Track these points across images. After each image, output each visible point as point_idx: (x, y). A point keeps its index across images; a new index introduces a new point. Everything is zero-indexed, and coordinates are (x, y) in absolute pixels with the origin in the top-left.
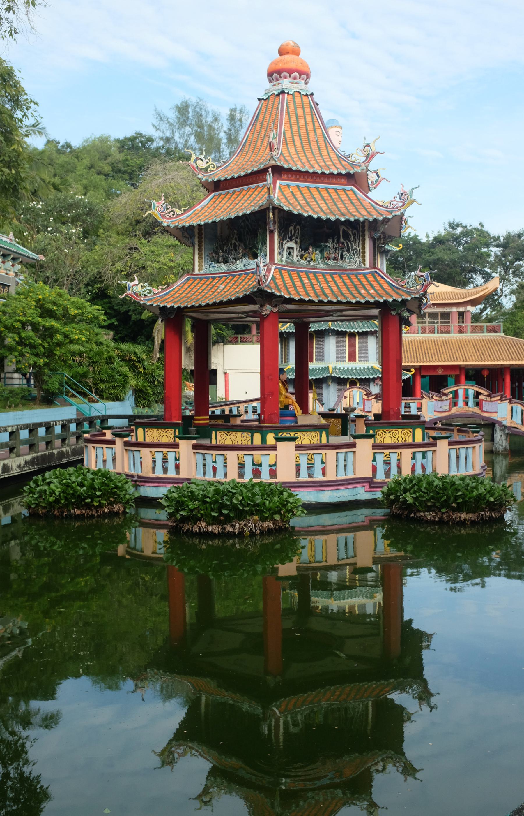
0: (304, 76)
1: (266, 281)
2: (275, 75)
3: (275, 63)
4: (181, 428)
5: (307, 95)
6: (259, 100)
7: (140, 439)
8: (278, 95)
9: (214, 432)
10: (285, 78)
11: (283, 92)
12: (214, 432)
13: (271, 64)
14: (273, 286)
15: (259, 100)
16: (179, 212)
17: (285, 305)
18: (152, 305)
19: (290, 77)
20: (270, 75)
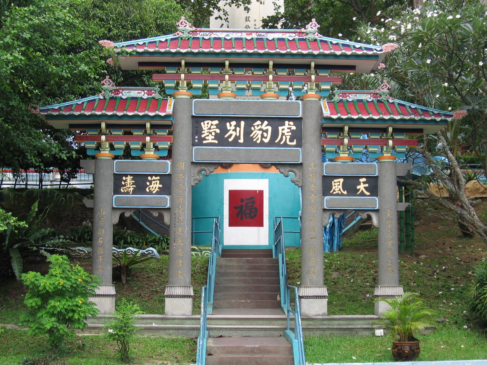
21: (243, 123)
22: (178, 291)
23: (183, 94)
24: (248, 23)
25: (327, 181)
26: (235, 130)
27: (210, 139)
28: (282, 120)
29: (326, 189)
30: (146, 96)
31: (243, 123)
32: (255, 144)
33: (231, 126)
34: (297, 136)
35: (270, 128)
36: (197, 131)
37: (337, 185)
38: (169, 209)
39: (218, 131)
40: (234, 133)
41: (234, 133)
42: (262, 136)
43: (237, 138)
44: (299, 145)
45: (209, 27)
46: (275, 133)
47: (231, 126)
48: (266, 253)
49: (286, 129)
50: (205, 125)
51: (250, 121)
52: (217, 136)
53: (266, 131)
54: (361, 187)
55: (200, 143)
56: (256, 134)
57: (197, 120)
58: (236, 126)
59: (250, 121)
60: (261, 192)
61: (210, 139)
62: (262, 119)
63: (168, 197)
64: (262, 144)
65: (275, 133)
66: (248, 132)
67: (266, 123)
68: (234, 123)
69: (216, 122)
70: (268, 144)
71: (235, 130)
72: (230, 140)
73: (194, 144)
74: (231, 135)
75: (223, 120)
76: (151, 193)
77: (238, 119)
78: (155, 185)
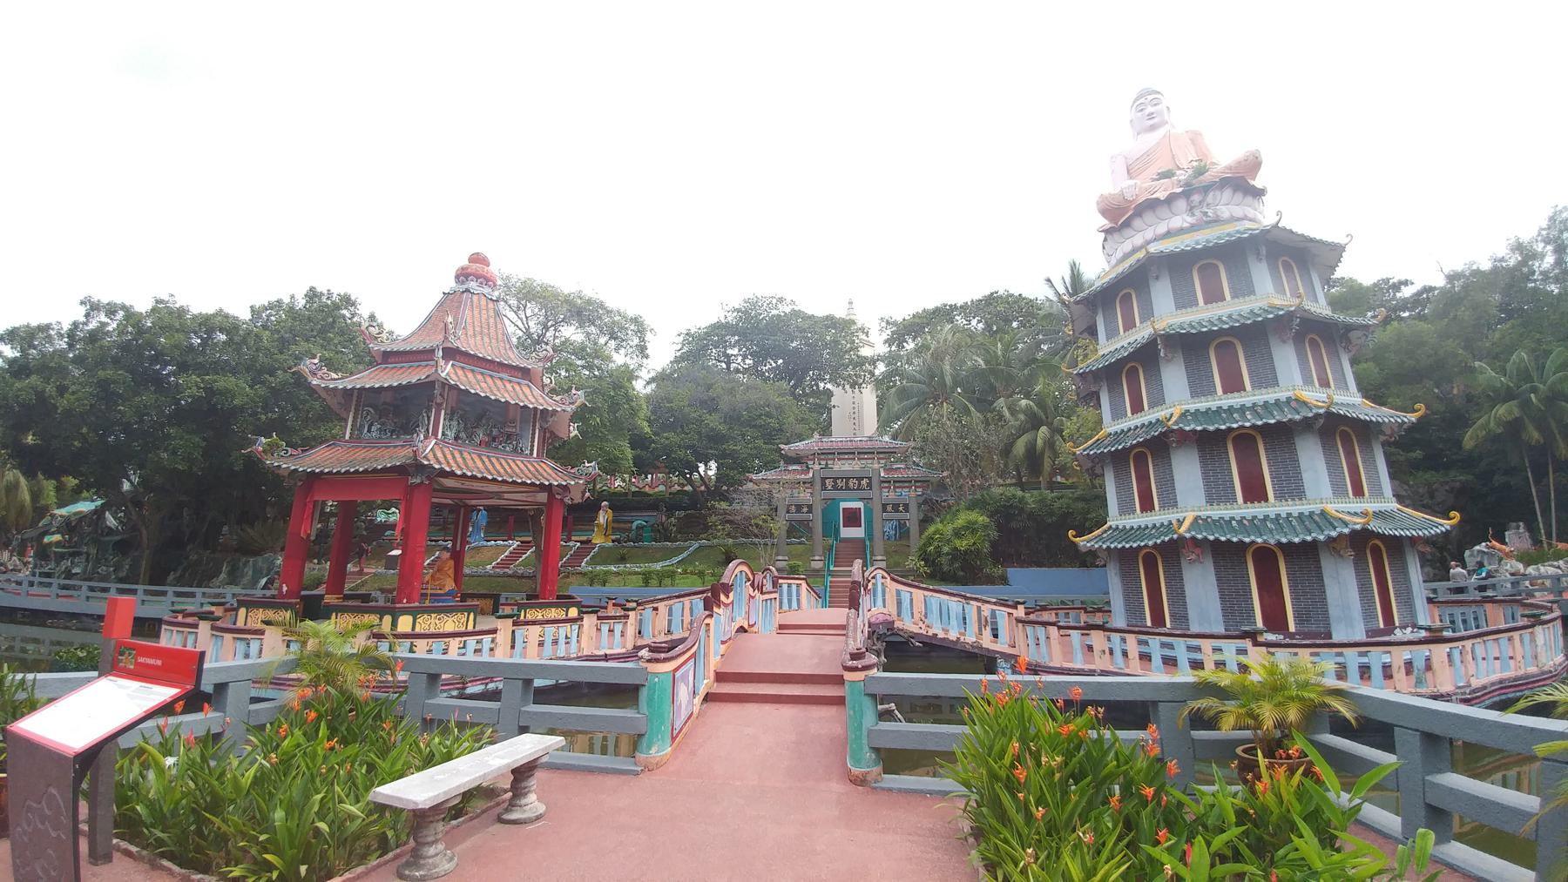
1: (425, 451)
5: (491, 299)
6: (444, 293)
7: (240, 624)
8: (463, 292)
9: (334, 614)
11: (467, 290)
12: (334, 614)
14: (431, 456)
15: (444, 293)
16: (336, 377)
17: (440, 479)
18: (279, 466)
20: (457, 277)
22: (817, 558)
23: (817, 467)
25: (884, 507)
27: (830, 488)
28: (862, 478)
29: (884, 510)
33: (839, 481)
34: (870, 485)
36: (823, 484)
37: (889, 508)
44: (871, 489)
45: (826, 430)
46: (860, 484)
47: (839, 481)
48: (862, 541)
49: (864, 482)
50: (827, 481)
54: (901, 508)
57: (823, 479)
61: (830, 488)
65: (860, 484)
66: (847, 483)
70: (858, 489)
78: (805, 510)
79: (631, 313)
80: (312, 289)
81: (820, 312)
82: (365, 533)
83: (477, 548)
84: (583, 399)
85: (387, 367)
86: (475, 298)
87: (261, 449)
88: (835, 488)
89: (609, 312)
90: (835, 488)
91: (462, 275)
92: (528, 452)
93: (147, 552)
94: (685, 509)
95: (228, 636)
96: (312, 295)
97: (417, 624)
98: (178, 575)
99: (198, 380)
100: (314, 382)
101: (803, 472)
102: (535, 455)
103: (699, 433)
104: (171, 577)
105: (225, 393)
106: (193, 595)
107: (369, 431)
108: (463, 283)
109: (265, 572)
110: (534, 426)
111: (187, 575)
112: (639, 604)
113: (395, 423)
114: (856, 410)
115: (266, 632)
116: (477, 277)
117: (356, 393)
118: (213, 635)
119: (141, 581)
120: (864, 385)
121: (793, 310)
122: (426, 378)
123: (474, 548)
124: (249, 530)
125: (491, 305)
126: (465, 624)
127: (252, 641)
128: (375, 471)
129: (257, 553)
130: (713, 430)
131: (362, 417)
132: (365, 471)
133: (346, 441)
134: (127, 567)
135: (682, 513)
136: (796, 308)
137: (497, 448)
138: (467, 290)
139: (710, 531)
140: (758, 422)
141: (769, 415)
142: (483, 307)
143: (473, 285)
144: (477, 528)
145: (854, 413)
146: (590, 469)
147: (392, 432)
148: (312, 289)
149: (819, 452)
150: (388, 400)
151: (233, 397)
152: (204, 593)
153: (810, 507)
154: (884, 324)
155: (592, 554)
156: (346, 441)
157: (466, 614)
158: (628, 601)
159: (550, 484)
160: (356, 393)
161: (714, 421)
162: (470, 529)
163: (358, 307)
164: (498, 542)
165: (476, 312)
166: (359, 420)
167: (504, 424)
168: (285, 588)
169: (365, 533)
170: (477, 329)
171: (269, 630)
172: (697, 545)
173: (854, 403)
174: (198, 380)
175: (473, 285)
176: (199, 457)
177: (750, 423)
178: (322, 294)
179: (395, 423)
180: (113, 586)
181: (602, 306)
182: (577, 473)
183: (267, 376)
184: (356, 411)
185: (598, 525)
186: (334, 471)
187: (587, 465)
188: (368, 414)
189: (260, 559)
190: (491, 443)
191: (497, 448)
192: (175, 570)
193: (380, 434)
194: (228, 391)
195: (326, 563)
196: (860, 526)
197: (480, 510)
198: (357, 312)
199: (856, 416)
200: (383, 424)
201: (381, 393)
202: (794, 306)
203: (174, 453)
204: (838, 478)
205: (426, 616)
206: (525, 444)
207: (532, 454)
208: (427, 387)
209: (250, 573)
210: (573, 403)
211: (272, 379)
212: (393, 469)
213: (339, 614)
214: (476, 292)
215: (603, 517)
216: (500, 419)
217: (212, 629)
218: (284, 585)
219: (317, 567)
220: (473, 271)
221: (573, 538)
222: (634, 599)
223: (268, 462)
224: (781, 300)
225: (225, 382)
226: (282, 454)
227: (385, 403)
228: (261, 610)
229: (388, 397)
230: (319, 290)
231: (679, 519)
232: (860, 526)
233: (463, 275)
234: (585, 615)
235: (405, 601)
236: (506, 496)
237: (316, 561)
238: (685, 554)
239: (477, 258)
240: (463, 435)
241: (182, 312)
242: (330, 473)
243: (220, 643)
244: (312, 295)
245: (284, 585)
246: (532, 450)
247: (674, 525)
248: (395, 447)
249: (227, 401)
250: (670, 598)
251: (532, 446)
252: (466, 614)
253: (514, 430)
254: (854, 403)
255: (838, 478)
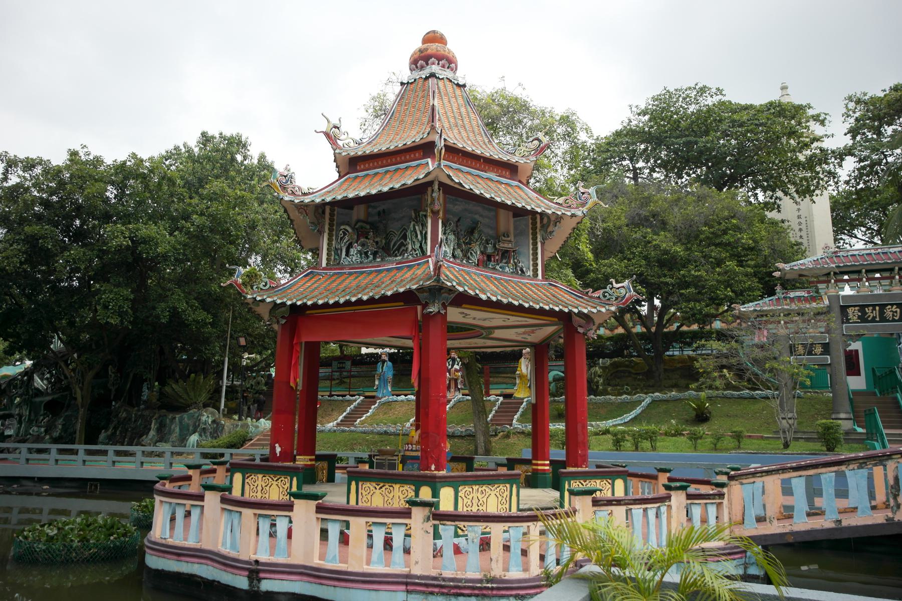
0: (453, 65)
2: (421, 62)
3: (421, 51)
4: (301, 475)
5: (458, 85)
6: (402, 84)
8: (427, 78)
10: (434, 64)
13: (415, 53)
15: (402, 84)
19: (438, 64)
21: (877, 308)
22: (842, 416)
24: (800, 220)
26: (872, 312)
30: (806, 295)
31: (877, 308)
32: (888, 321)
35: (898, 310)
38: (830, 364)
39: (860, 314)
40: (872, 315)
41: (872, 315)
42: (893, 315)
43: (874, 318)
50: (850, 311)
51: (883, 307)
52: (859, 317)
53: (896, 312)
55: (848, 321)
56: (888, 313)
58: (872, 310)
59: (883, 307)
60: (857, 351)
62: (892, 305)
63: (828, 357)
64: (894, 320)
67: (895, 307)
68: (871, 308)
69: (857, 308)
71: (872, 312)
72: (869, 319)
73: (843, 323)
74: (869, 316)
75: (862, 308)
76: (816, 354)
77: (874, 306)
79: (559, 111)
80: (204, 134)
81: (759, 100)
82: (265, 388)
83: (389, 403)
84: (596, 198)
85: (357, 177)
86: (441, 83)
87: (240, 281)
88: (863, 319)
89: (533, 114)
90: (863, 319)
91: (421, 58)
92: (530, 273)
93: (81, 411)
94: (610, 356)
95: (248, 513)
96: (206, 139)
97: (459, 498)
98: (109, 432)
99: (123, 228)
100: (286, 199)
101: (813, 299)
102: (540, 277)
103: (646, 258)
104: (103, 436)
105: (146, 241)
106: (132, 454)
107: (347, 254)
108: (422, 68)
109: (191, 428)
110: (535, 239)
111: (118, 433)
112: (731, 478)
113: (377, 243)
114: (803, 227)
115: (295, 507)
116: (439, 58)
117: (328, 209)
118: (223, 509)
119: (77, 440)
120: (817, 192)
121: (722, 103)
122: (425, 176)
123: (384, 404)
124: (174, 386)
125: (458, 91)
126: (508, 499)
127: (278, 519)
128: (360, 302)
129: (183, 408)
130: (666, 252)
131: (337, 239)
132: (372, 300)
133: (324, 269)
134: (60, 427)
135: (608, 361)
136: (724, 99)
137: (494, 269)
138: (433, 75)
139: (702, 380)
140: (726, 238)
141: (737, 229)
142: (451, 95)
143: (435, 68)
144: (384, 382)
145: (800, 230)
146: (623, 291)
147: (375, 254)
148: (204, 134)
149: (837, 271)
150: (362, 216)
151: (157, 244)
152: (143, 452)
153: (826, 349)
154: (852, 105)
155: (521, 410)
156: (324, 269)
157: (508, 486)
158: (717, 474)
159: (570, 311)
160: (328, 209)
161: (664, 241)
162: (377, 383)
163: (249, 148)
164: (409, 396)
165: (446, 101)
166: (334, 243)
167: (497, 239)
168: (278, 450)
169: (265, 388)
170: (452, 120)
171: (299, 504)
172: (648, 400)
173: (799, 217)
174: (123, 228)
175: (435, 68)
176: (130, 311)
177: (714, 241)
178: (213, 137)
179: (377, 243)
180: (54, 447)
181: (524, 107)
182: (601, 297)
183: (184, 222)
184: (331, 230)
185: (521, 376)
186: (331, 302)
187: (615, 285)
188: (345, 234)
189: (185, 416)
190: (486, 260)
191: (494, 269)
192: (106, 429)
193: (361, 257)
194: (151, 239)
195: (246, 419)
196: (859, 374)
197: (384, 361)
198: (248, 153)
199: (803, 233)
200: (363, 245)
201: (351, 208)
202: (720, 97)
203: (106, 307)
204: (868, 306)
205: (467, 488)
206: (526, 263)
207: (535, 274)
208: (420, 190)
209: (177, 430)
210: (583, 205)
211: (189, 225)
212: (396, 297)
213: (360, 484)
214: (441, 77)
215: (525, 367)
216: (491, 232)
217: (317, 512)
218: (277, 445)
219: (240, 423)
220: (434, 51)
221: (492, 392)
222: (725, 470)
223: (249, 296)
224: (703, 90)
225: (147, 230)
226: (261, 286)
227: (358, 221)
228: (260, 476)
229: (359, 212)
230: (210, 134)
231: (604, 368)
232: (859, 374)
233: (420, 60)
234: (672, 493)
235: (433, 467)
236: (498, 334)
237: (236, 417)
238: (638, 410)
239: (433, 38)
240: (458, 252)
241: (98, 161)
242: (315, 306)
243: (236, 522)
244: (206, 139)
245: (277, 445)
246: (535, 271)
247: (599, 376)
248: (388, 270)
249: (151, 249)
250: (784, 470)
251: (535, 265)
252: (508, 486)
253: (510, 245)
254: (799, 217)
255: (868, 306)
